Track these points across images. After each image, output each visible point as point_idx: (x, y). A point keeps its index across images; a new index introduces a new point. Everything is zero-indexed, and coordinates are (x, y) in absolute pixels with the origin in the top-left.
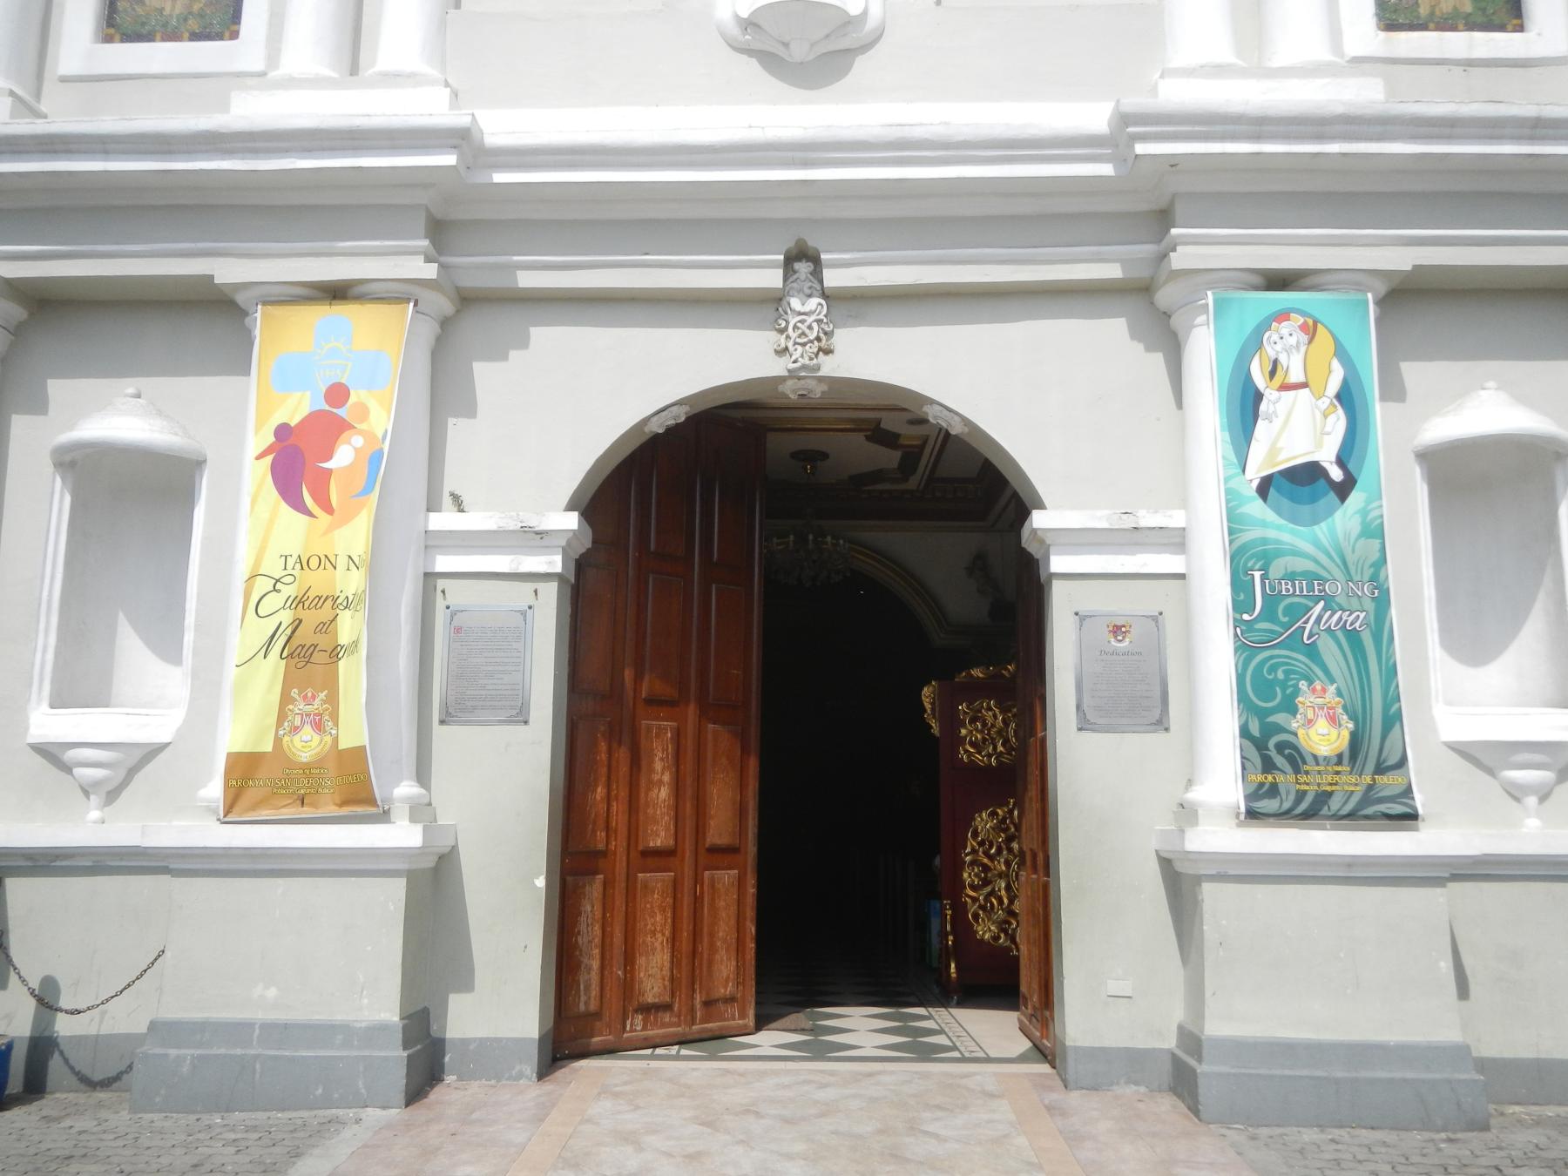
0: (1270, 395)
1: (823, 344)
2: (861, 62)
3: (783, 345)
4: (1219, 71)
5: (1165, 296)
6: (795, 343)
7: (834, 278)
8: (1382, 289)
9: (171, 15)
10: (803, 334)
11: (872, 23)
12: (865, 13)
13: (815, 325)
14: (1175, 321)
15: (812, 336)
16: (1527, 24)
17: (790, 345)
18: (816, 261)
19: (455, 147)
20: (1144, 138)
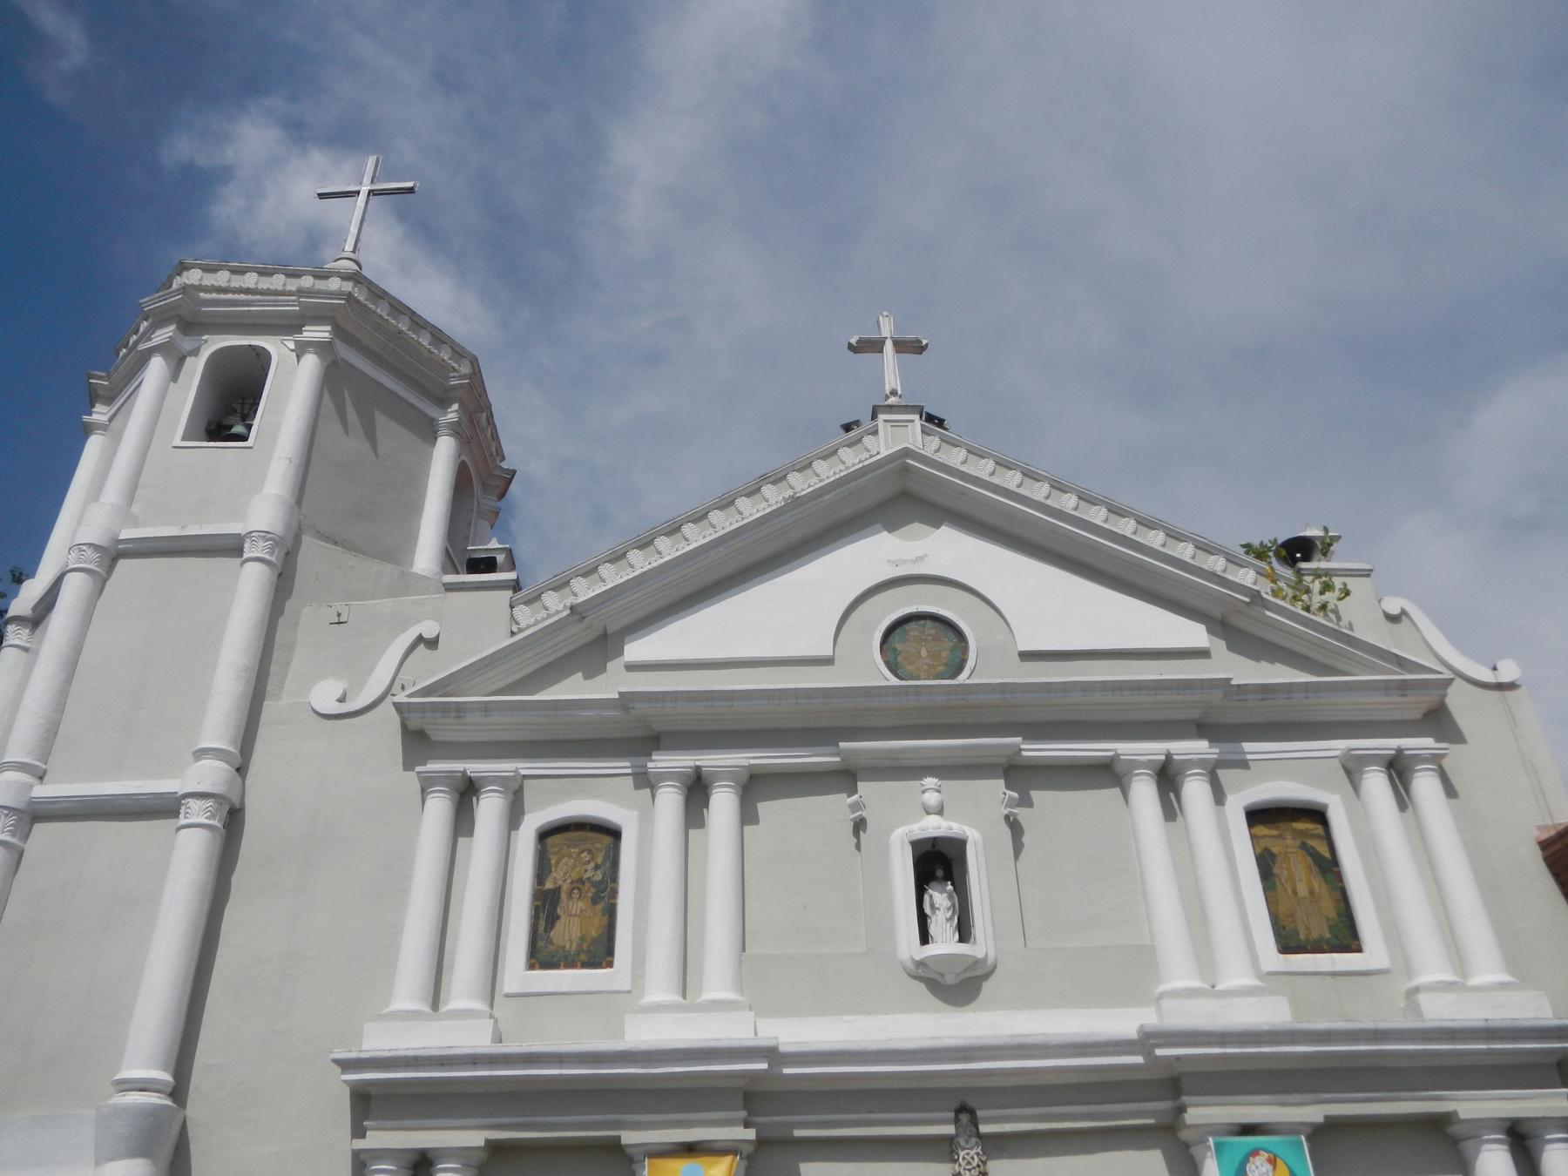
1: (982, 1168)
2: (987, 987)
3: (957, 1171)
4: (1193, 993)
5: (1185, 1135)
6: (965, 1169)
7: (984, 1129)
8: (1309, 1130)
9: (569, 951)
10: (969, 1163)
11: (990, 961)
12: (987, 955)
13: (976, 1157)
14: (1194, 1150)
15: (975, 1164)
16: (1364, 948)
17: (962, 1171)
18: (972, 1112)
19: (767, 1057)
20: (1159, 1046)
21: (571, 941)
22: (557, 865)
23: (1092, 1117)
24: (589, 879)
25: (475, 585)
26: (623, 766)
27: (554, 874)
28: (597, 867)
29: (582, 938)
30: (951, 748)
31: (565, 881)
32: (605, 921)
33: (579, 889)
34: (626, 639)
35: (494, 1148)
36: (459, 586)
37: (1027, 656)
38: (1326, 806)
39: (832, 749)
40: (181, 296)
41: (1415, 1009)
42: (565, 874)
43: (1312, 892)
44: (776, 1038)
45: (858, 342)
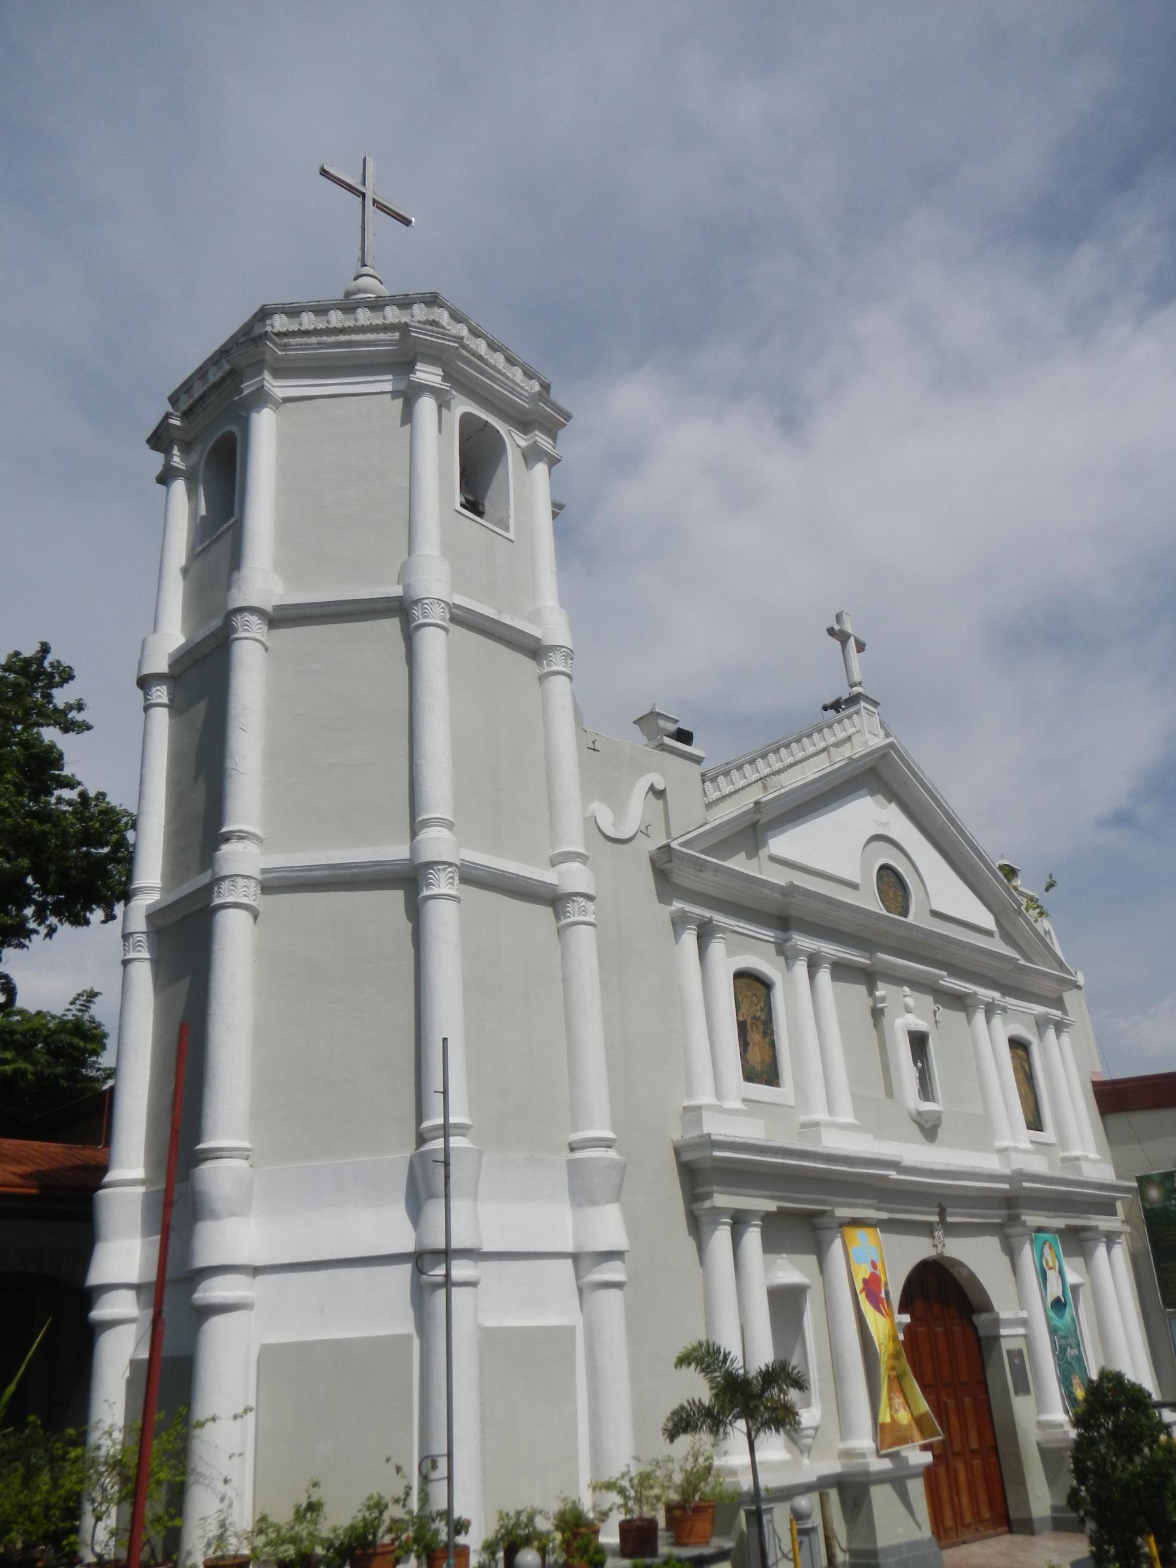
0: (1048, 1272)
7: (949, 1219)
21: (757, 1063)
22: (742, 1000)
23: (982, 1216)
24: (759, 1017)
25: (681, 753)
26: (769, 934)
27: (742, 1009)
28: (762, 1010)
29: (763, 1062)
30: (919, 970)
31: (748, 1016)
32: (771, 1053)
33: (756, 1025)
34: (769, 834)
35: (781, 1213)
36: (672, 749)
37: (935, 914)
38: (1031, 1043)
39: (867, 955)
40: (456, 345)
41: (1079, 1170)
42: (747, 1010)
43: (1026, 1094)
44: (902, 1157)
45: (839, 631)
